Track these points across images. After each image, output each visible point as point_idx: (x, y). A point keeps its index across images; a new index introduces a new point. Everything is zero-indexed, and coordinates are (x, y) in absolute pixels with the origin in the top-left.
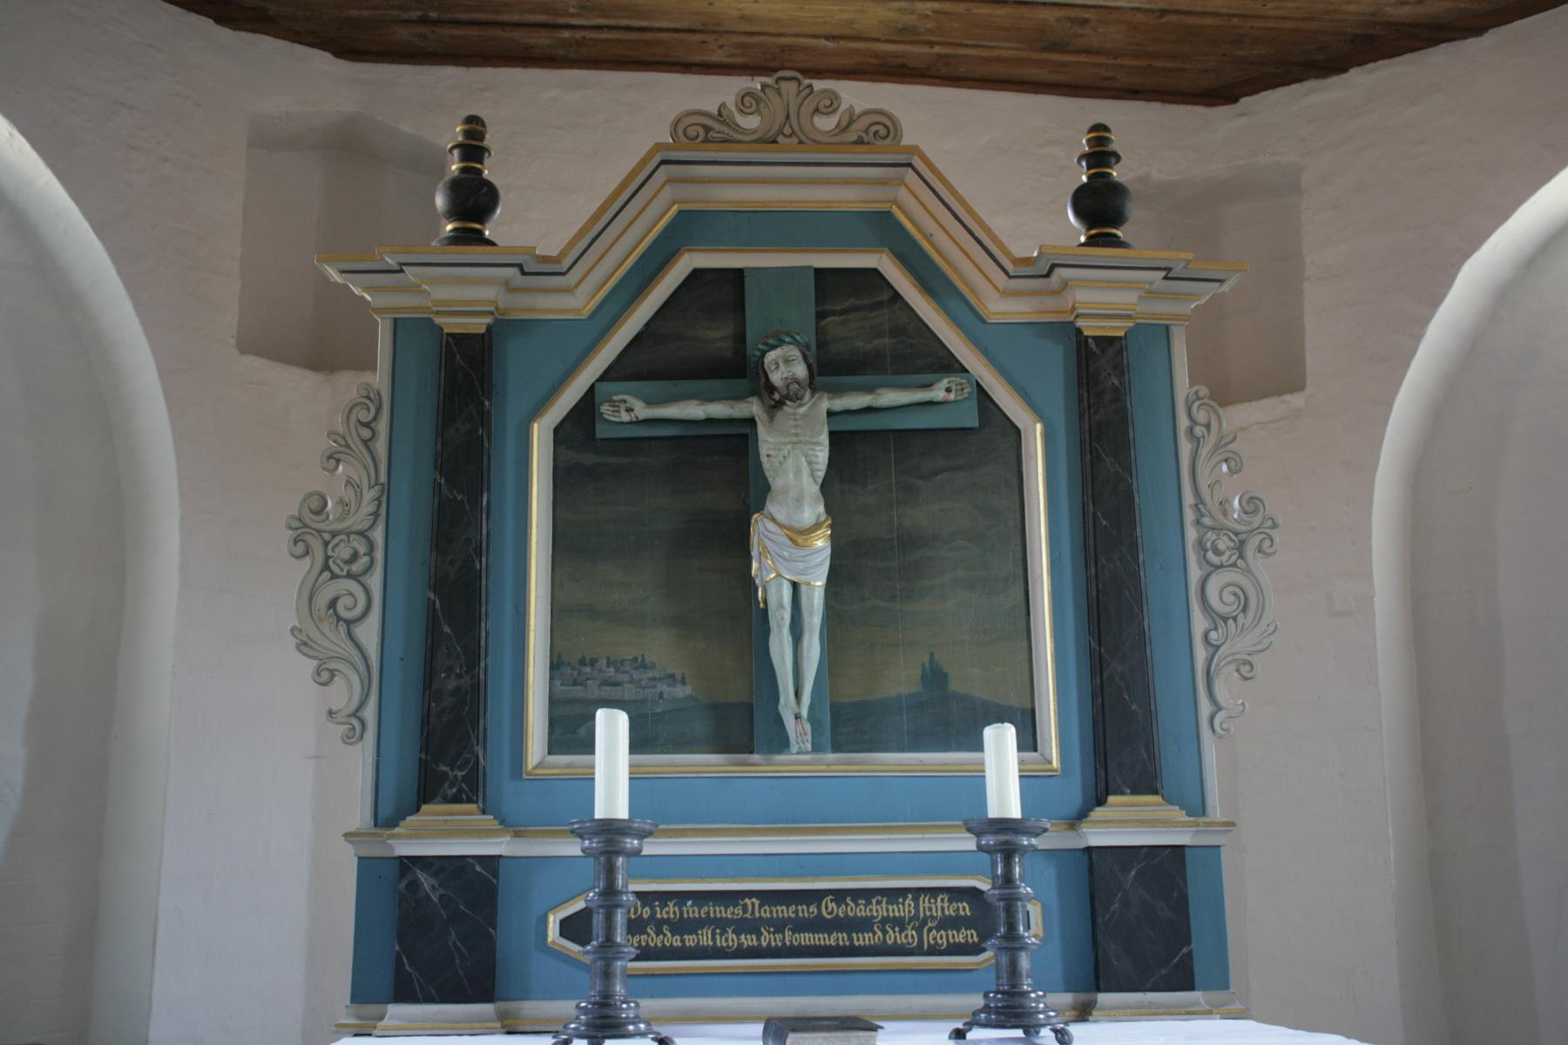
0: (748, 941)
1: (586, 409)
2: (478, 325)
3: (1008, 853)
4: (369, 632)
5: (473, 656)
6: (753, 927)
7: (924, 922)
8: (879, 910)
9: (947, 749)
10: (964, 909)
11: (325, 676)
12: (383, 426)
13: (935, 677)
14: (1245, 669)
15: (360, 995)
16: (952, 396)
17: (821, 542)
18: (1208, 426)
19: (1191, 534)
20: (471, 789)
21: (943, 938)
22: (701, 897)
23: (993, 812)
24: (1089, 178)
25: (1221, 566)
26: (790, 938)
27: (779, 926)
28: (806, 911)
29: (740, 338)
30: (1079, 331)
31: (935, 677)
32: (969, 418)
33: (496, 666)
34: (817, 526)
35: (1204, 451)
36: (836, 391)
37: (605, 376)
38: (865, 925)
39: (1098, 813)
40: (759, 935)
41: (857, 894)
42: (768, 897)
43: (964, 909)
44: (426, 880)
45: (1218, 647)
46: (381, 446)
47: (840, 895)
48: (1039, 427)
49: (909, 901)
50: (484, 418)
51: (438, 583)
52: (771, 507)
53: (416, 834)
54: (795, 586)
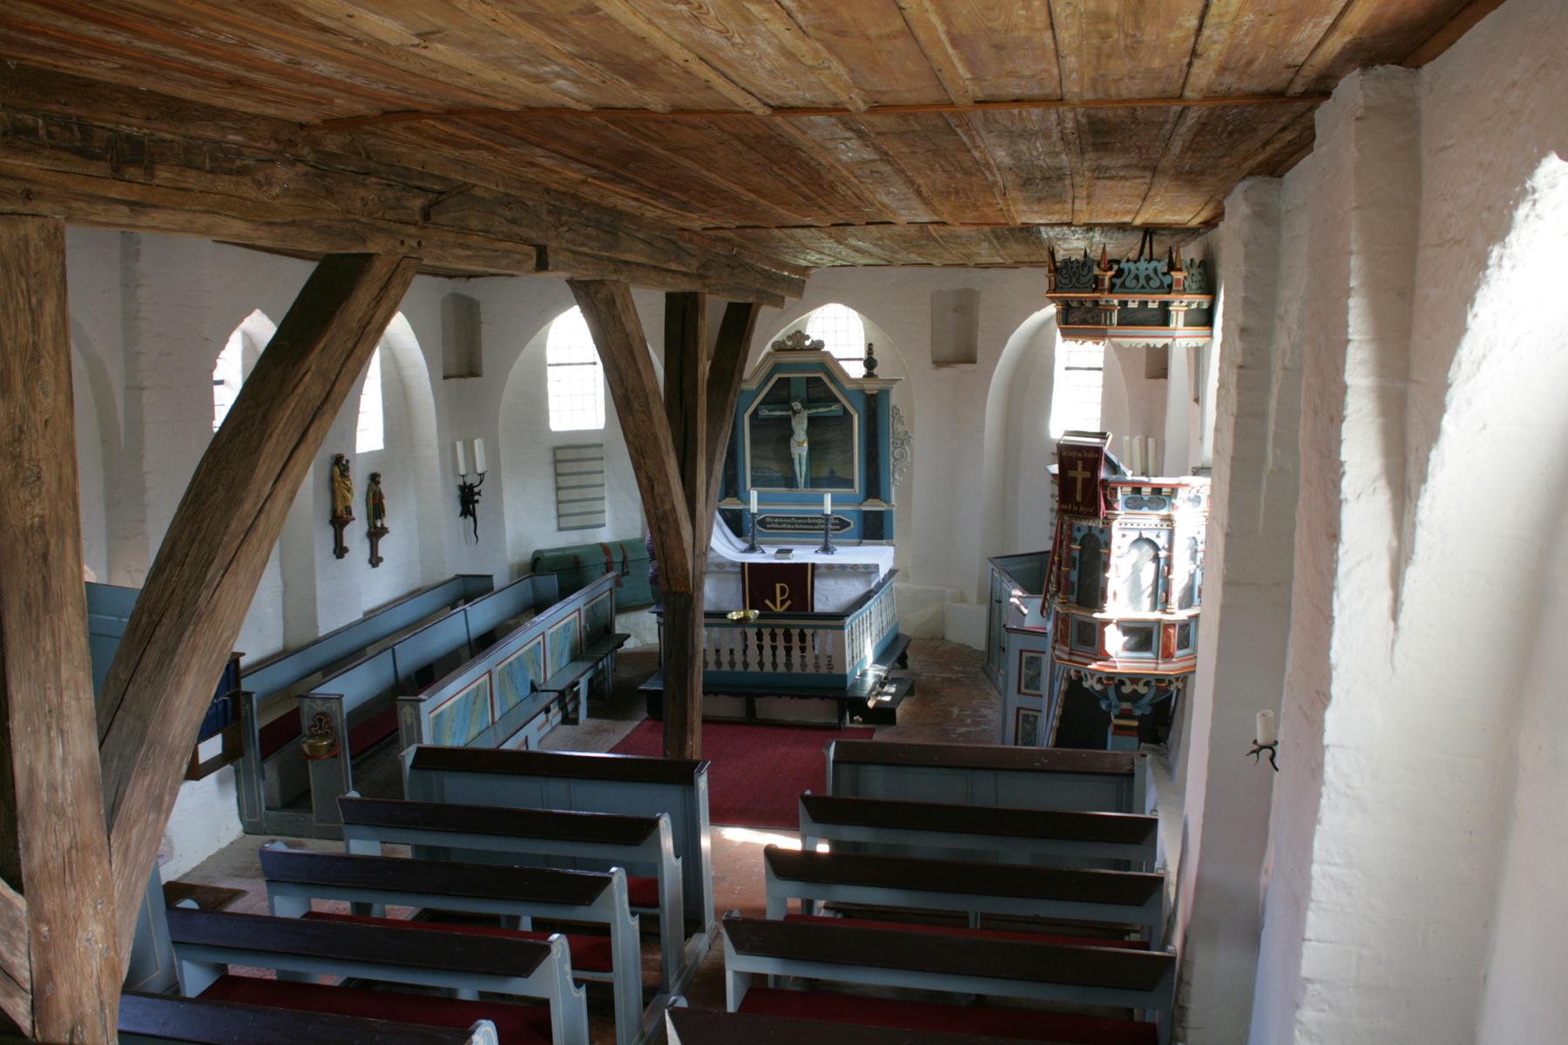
1: (755, 412)
6: (794, 524)
13: (832, 472)
17: (806, 445)
19: (891, 440)
22: (783, 518)
26: (801, 526)
27: (799, 524)
31: (832, 472)
32: (841, 413)
36: (809, 409)
37: (761, 403)
38: (817, 524)
42: (797, 518)
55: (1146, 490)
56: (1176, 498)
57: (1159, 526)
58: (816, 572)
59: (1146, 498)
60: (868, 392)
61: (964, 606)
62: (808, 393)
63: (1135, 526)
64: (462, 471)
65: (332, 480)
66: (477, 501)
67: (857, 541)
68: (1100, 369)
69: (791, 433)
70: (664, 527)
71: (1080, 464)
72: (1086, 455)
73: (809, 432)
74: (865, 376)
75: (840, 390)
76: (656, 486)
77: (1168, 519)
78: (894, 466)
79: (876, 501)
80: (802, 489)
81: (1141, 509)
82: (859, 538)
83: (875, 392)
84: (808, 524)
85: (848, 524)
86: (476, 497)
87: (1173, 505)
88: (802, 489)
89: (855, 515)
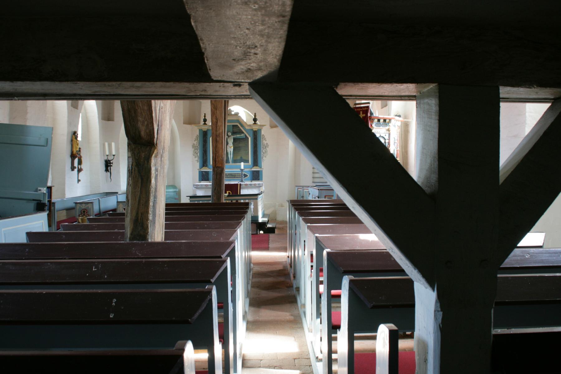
0: (227, 177)
2: (206, 130)
3: (242, 171)
4: (198, 154)
5: (206, 156)
6: (227, 176)
8: (237, 175)
11: (195, 157)
12: (199, 138)
13: (241, 158)
15: (199, 181)
17: (232, 148)
19: (262, 146)
20: (207, 166)
26: (230, 177)
27: (229, 176)
28: (231, 175)
31: (241, 158)
32: (245, 137)
33: (208, 156)
34: (232, 146)
36: (234, 135)
38: (236, 176)
39: (253, 168)
41: (235, 174)
42: (229, 174)
44: (204, 173)
46: (199, 139)
47: (234, 174)
48: (250, 138)
50: (206, 137)
51: (204, 151)
53: (203, 169)
54: (230, 151)
55: (382, 121)
56: (390, 123)
57: (386, 132)
58: (241, 186)
59: (381, 123)
60: (254, 130)
61: (284, 208)
62: (233, 131)
63: (378, 132)
64: (107, 153)
65: (72, 141)
66: (112, 166)
67: (250, 181)
70: (218, 139)
71: (361, 112)
72: (363, 109)
73: (233, 143)
74: (253, 124)
75: (244, 129)
76: (218, 122)
77: (388, 130)
78: (263, 155)
79: (257, 167)
80: (231, 164)
81: (380, 127)
82: (251, 180)
83: (256, 130)
84: (232, 176)
85: (247, 176)
86: (111, 164)
87: (390, 126)
88: (231, 164)
89: (249, 172)
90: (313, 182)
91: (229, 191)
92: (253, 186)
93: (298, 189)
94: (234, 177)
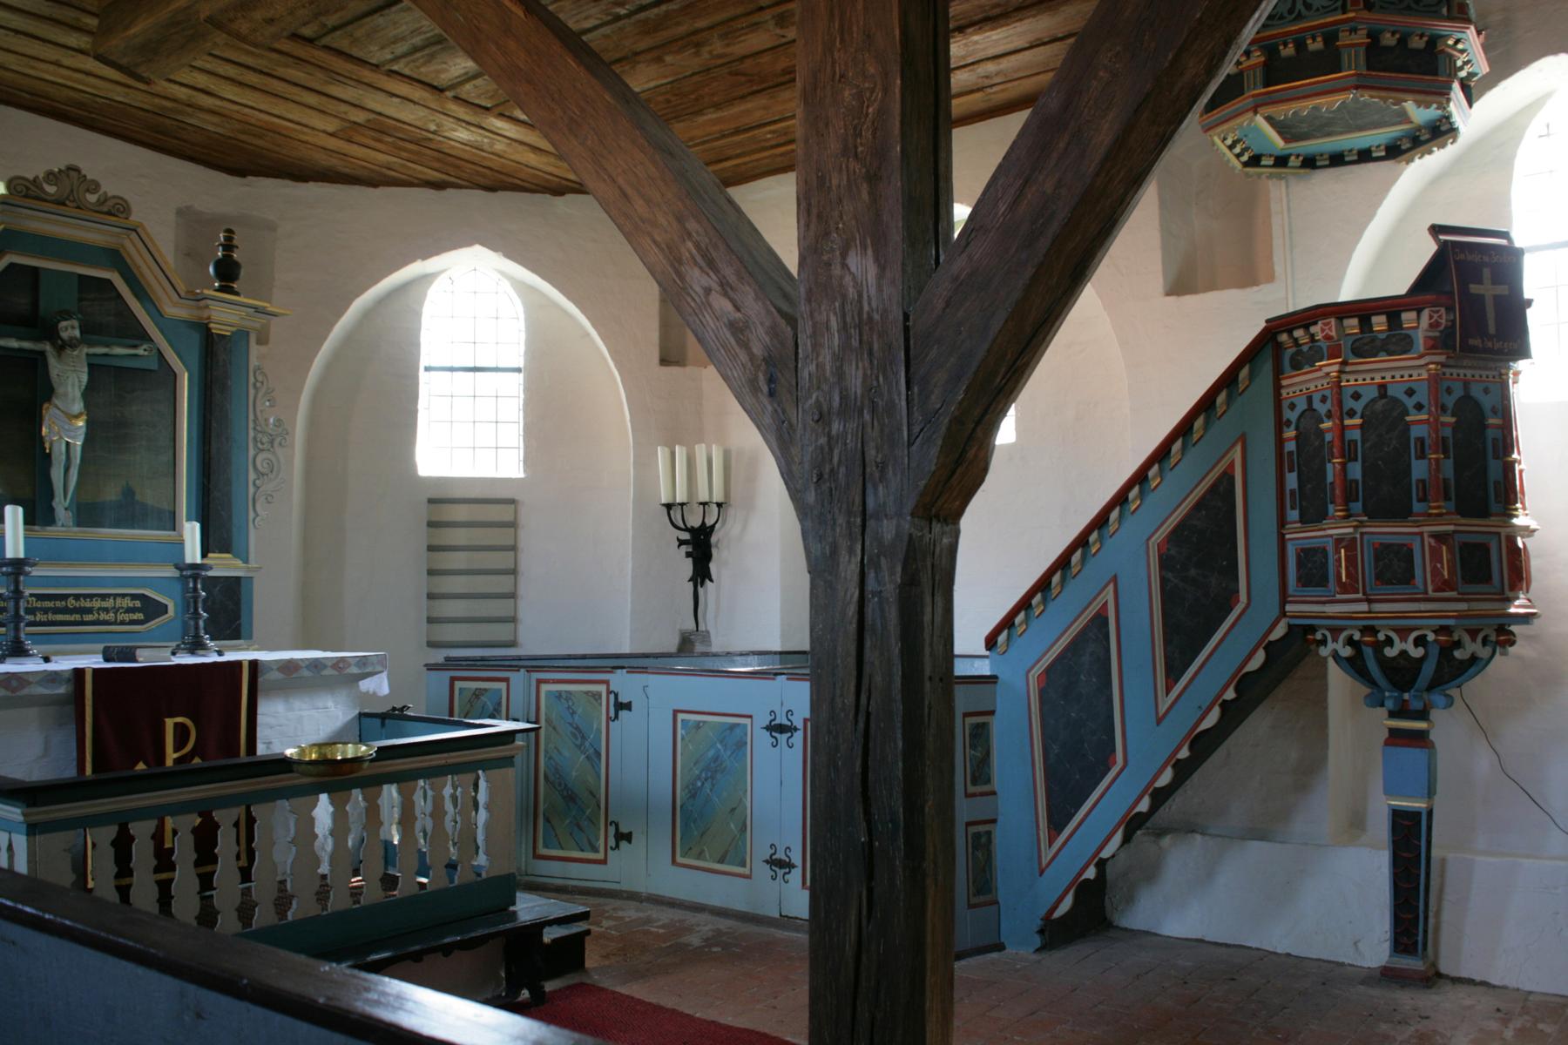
7: (118, 610)
8: (97, 604)
9: (133, 528)
10: (138, 604)
14: (269, 498)
16: (146, 353)
18: (262, 383)
19: (252, 434)
21: (127, 617)
23: (189, 560)
24: (223, 255)
25: (263, 450)
26: (51, 617)
27: (45, 611)
28: (59, 604)
29: (35, 304)
30: (209, 330)
31: (129, 493)
35: (260, 395)
36: (91, 344)
38: (90, 611)
40: (35, 615)
41: (86, 596)
43: (138, 604)
45: (258, 488)
47: (77, 597)
48: (186, 375)
49: (112, 600)
52: (56, 401)
68: (518, 370)
69: (45, 391)
73: (89, 393)
85: (165, 609)
90: (432, 644)
91: (179, 719)
92: (325, 672)
93: (453, 679)
94: (77, 617)
